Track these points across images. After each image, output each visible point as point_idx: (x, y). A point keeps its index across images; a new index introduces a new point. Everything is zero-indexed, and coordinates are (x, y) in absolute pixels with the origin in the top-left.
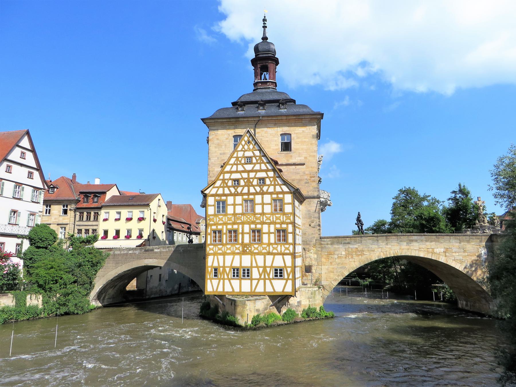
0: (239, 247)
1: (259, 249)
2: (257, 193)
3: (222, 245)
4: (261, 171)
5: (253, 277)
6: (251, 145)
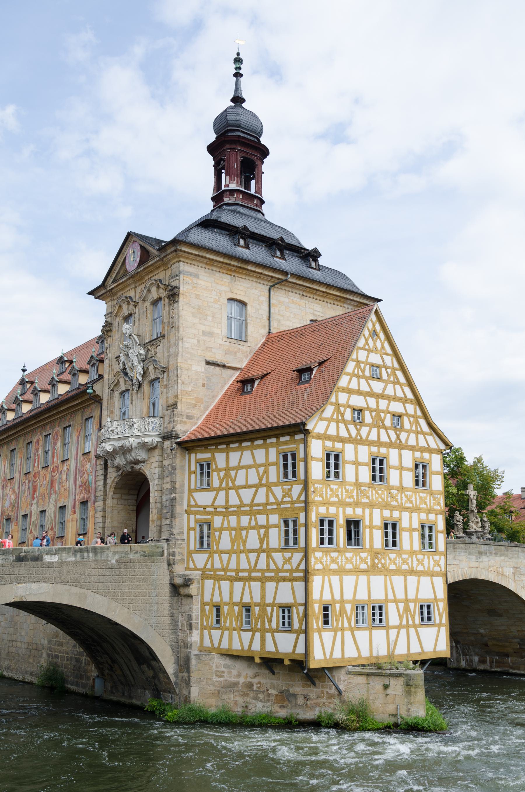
0: (366, 558)
1: (397, 562)
2: (390, 445)
3: (336, 550)
4: (396, 399)
5: (391, 623)
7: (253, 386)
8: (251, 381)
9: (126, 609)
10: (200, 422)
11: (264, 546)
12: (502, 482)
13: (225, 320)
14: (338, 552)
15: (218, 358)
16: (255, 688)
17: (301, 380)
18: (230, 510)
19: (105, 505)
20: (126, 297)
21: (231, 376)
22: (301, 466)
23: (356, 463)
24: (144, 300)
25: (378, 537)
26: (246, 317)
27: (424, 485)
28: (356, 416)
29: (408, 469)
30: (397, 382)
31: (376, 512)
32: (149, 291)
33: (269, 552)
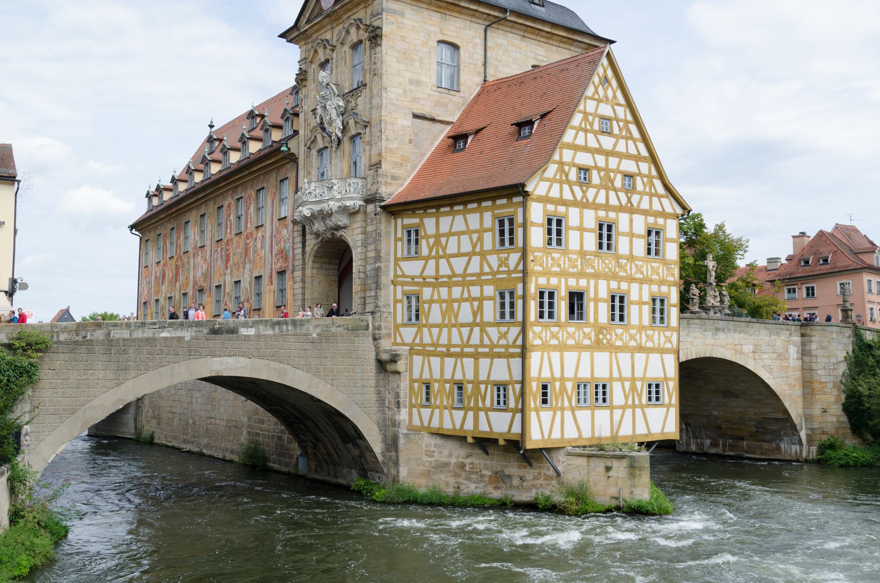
0: (590, 333)
1: (624, 338)
2: (620, 209)
3: (556, 325)
4: (629, 156)
5: (615, 403)
6: (610, 89)
7: (466, 143)
8: (464, 137)
9: (329, 386)
10: (406, 183)
11: (478, 320)
12: (745, 251)
13: (434, 66)
14: (559, 326)
15: (426, 109)
16: (467, 468)
17: (520, 135)
18: (440, 280)
19: (304, 275)
20: (322, 40)
21: (441, 132)
22: (519, 232)
23: (581, 229)
24: (342, 44)
25: (604, 310)
26: (458, 62)
27: (657, 253)
28: (582, 176)
29: (639, 236)
30: (629, 137)
31: (603, 284)
32: (348, 32)
33: (483, 326)
